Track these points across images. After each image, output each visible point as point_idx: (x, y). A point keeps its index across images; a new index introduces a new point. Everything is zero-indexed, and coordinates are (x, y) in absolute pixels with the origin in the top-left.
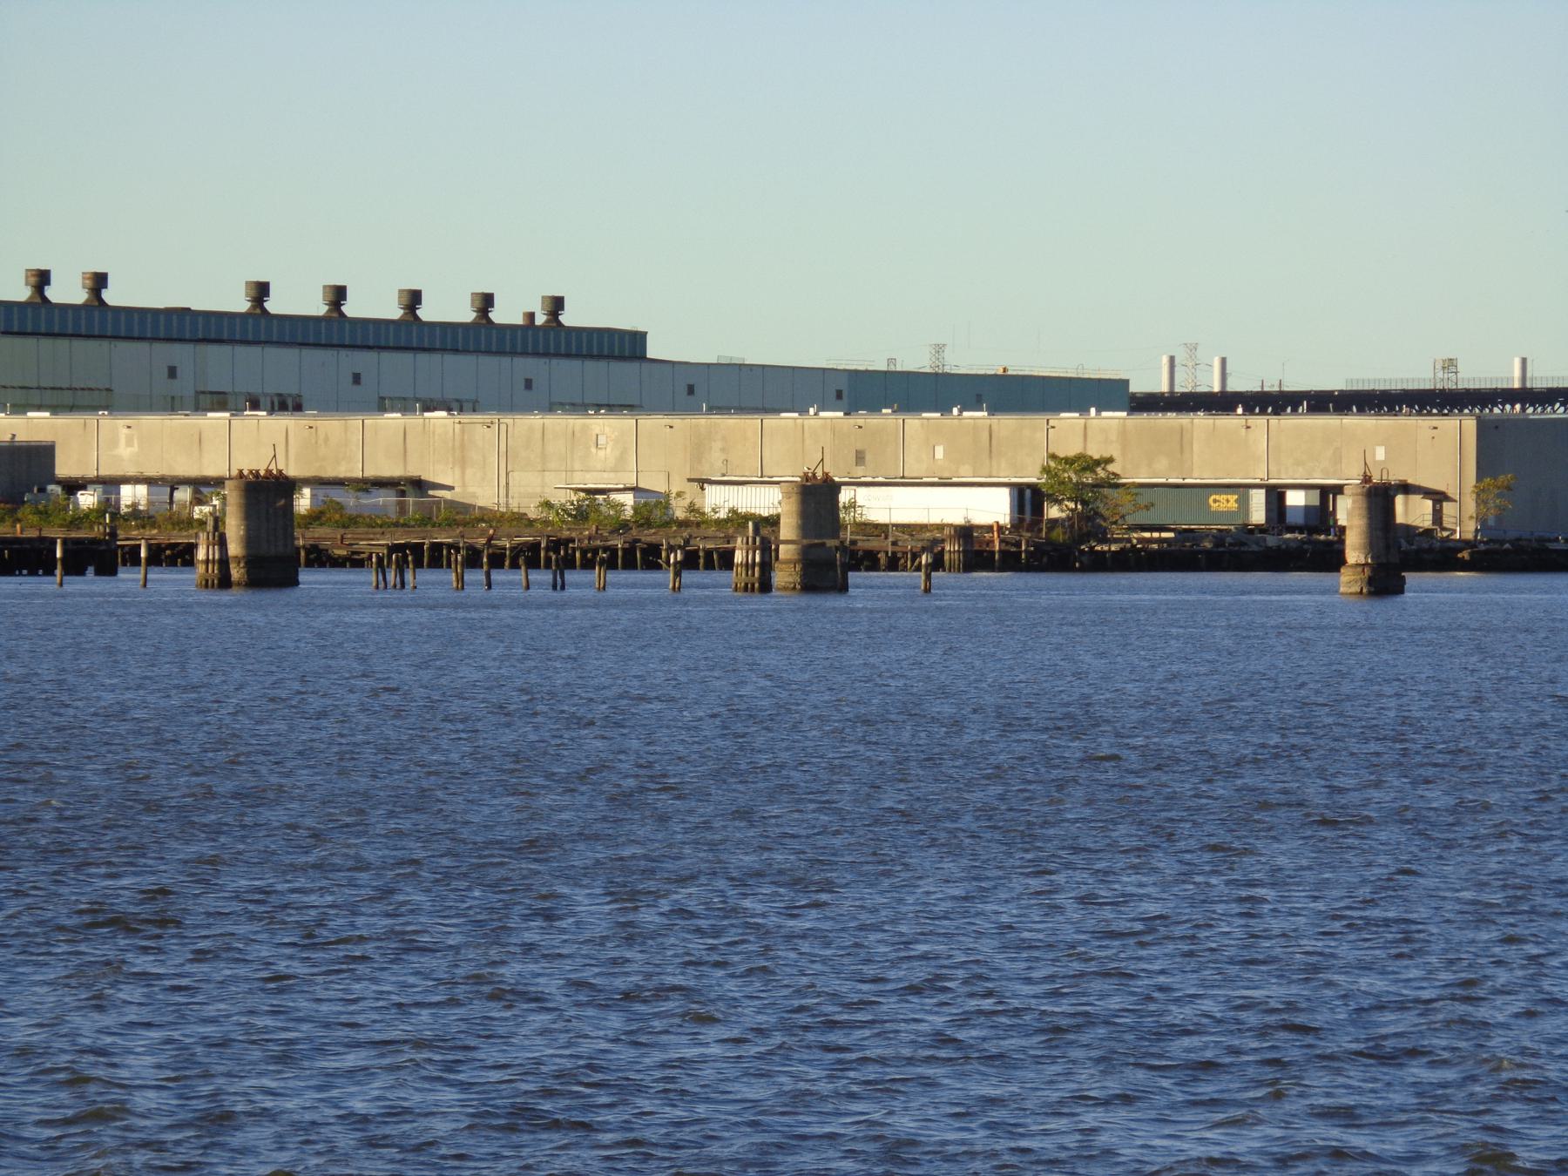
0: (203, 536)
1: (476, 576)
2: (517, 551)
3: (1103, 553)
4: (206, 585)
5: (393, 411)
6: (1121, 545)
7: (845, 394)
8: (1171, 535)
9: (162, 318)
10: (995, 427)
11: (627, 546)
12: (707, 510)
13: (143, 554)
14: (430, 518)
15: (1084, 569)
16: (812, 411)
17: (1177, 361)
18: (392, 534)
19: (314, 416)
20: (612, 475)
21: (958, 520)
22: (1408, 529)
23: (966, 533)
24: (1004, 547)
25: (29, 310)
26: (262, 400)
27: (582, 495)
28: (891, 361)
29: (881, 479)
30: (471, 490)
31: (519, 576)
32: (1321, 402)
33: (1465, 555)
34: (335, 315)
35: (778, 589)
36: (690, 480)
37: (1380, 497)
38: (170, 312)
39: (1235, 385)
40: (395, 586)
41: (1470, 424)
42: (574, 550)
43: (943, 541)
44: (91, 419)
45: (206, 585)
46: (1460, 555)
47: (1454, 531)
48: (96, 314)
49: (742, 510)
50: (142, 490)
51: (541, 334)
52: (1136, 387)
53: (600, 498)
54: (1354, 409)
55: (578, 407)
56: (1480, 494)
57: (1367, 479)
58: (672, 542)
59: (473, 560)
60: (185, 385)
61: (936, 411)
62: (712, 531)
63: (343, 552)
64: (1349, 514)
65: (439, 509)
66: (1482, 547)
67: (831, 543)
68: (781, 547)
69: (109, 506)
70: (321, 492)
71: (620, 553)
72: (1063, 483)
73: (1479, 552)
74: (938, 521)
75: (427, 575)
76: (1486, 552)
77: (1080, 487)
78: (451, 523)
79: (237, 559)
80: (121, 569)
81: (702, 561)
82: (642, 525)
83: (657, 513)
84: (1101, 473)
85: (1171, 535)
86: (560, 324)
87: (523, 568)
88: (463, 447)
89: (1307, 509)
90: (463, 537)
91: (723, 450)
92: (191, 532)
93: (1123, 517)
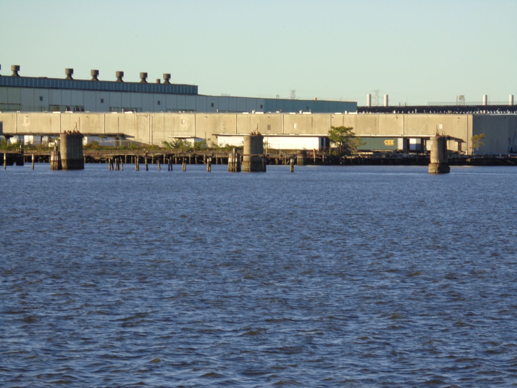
0: (52, 153)
1: (143, 166)
2: (156, 158)
3: (349, 159)
4: (54, 169)
5: (114, 111)
6: (355, 157)
7: (263, 106)
8: (371, 153)
9: (38, 80)
10: (314, 118)
11: (192, 156)
12: (219, 145)
13: (33, 158)
14: (127, 147)
15: (343, 164)
16: (253, 112)
17: (372, 96)
18: (115, 152)
19: (88, 113)
20: (187, 133)
21: (301, 148)
22: (451, 152)
23: (304, 152)
24: (317, 157)
25: (67, 82)
26: (71, 108)
27: (177, 139)
28: (277, 96)
29: (276, 135)
30: (140, 137)
31: (157, 166)
32: (421, 110)
33: (469, 160)
34: (95, 80)
35: (243, 171)
36: (213, 135)
37: (442, 141)
38: (40, 79)
39: (391, 104)
40: (116, 169)
41: (471, 117)
42: (175, 158)
43: (297, 155)
44: (14, 114)
45: (54, 169)
46: (467, 160)
47: (465, 152)
48: (16, 79)
49: (230, 145)
50: (31, 138)
51: (163, 86)
52: (359, 105)
53: (183, 140)
54: (430, 112)
55: (176, 110)
56: (474, 140)
57: (438, 135)
58: (208, 155)
59: (141, 161)
60: (45, 103)
61: (293, 112)
62: (220, 151)
63: (98, 158)
64: (432, 147)
65: (130, 144)
66: (474, 158)
67: (260, 155)
68: (244, 157)
69: (20, 142)
70: (91, 138)
71: (190, 159)
72: (336, 136)
73: (474, 159)
74: (295, 149)
75: (127, 166)
76: (476, 159)
77: (342, 137)
78: (134, 149)
79: (64, 160)
80: (25, 163)
81: (217, 161)
82: (197, 149)
83: (202, 145)
84: (348, 132)
85: (371, 153)
86: (169, 83)
87: (159, 163)
88: (137, 124)
89: (417, 145)
90: (138, 153)
91: (224, 125)
92: (48, 151)
93: (356, 147)
